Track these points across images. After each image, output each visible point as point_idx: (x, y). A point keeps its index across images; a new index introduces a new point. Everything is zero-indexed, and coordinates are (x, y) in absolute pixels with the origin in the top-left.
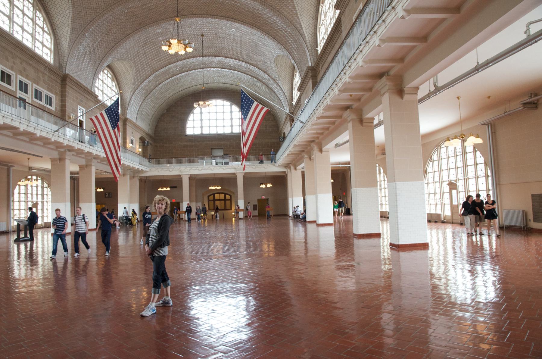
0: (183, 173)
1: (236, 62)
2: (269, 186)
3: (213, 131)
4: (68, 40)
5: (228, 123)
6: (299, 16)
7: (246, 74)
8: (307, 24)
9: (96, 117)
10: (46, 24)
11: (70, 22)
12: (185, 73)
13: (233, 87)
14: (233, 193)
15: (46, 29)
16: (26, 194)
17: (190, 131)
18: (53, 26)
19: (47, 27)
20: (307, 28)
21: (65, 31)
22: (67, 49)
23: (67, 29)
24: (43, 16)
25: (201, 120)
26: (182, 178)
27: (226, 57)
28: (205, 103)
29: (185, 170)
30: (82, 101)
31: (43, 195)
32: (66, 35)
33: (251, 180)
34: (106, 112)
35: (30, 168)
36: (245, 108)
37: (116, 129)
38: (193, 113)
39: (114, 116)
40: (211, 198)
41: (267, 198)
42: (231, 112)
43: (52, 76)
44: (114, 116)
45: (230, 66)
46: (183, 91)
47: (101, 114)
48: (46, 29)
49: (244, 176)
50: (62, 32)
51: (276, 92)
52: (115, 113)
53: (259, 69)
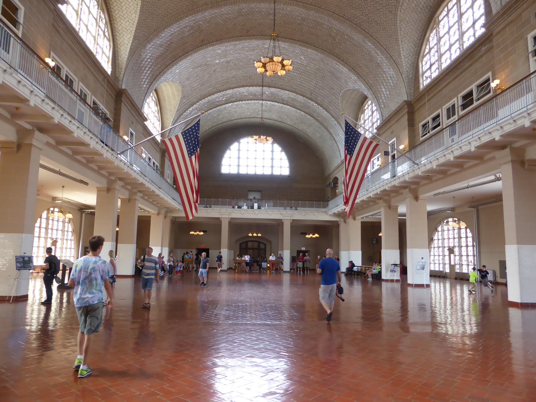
0: (223, 216)
1: (292, 95)
2: (317, 235)
3: (251, 171)
4: (129, 49)
5: (268, 163)
6: (400, 42)
7: (299, 109)
8: (407, 53)
9: (170, 140)
11: (134, 29)
12: (230, 104)
13: (278, 123)
14: (270, 242)
15: (107, 34)
16: (47, 228)
18: (114, 31)
19: (108, 31)
20: (406, 56)
21: (126, 38)
22: (126, 59)
23: (129, 36)
24: (105, 18)
26: (221, 222)
27: (282, 89)
28: (260, 137)
29: (225, 213)
30: (133, 123)
31: (63, 231)
32: (126, 42)
33: (300, 229)
34: (183, 135)
35: (54, 199)
36: (351, 142)
37: (193, 157)
39: (192, 141)
40: (244, 246)
41: (307, 249)
42: (272, 151)
43: (109, 90)
44: (192, 141)
45: (283, 100)
46: (222, 125)
47: (177, 137)
48: (107, 34)
49: (291, 224)
50: (122, 39)
51: (332, 132)
52: (193, 137)
53: (318, 104)
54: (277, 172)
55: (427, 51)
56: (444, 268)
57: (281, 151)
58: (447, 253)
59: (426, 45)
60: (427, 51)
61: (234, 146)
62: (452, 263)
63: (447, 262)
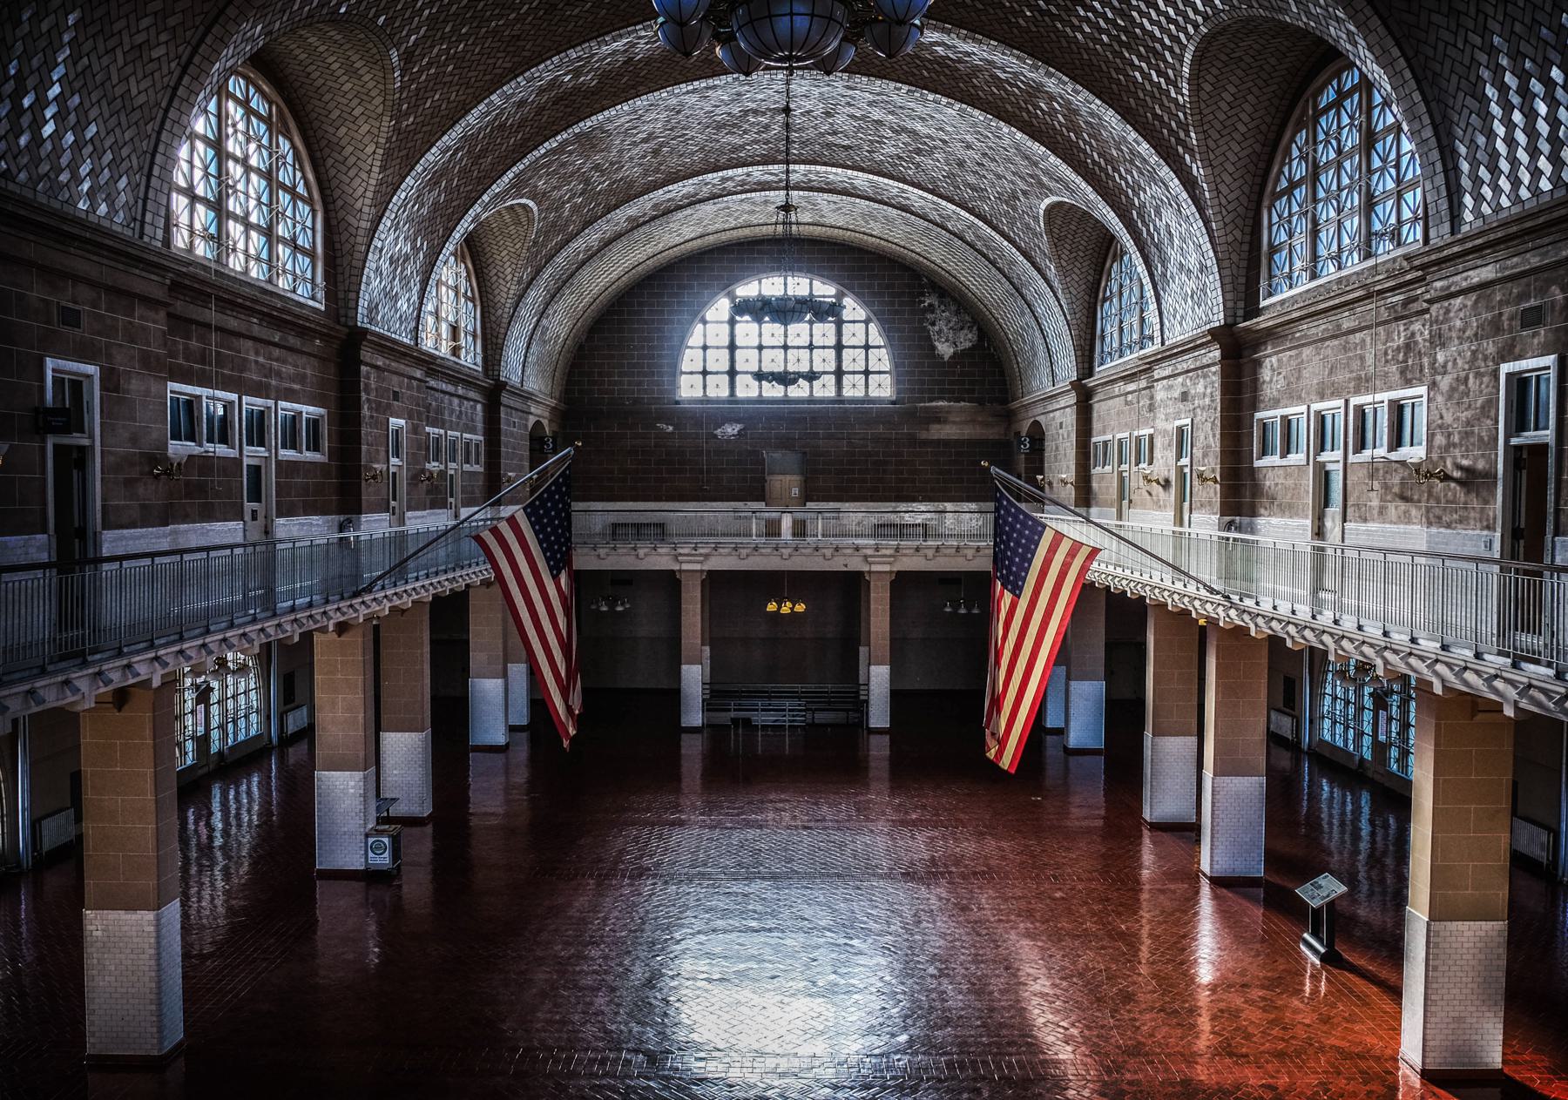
10: (302, 170)
17: (688, 389)
25: (732, 347)
38: (705, 322)
54: (853, 389)
55: (1284, 184)
56: (1358, 745)
57: (867, 322)
58: (1368, 702)
59: (1283, 164)
60: (1284, 184)
61: (721, 308)
62: (1382, 738)
63: (1368, 729)
